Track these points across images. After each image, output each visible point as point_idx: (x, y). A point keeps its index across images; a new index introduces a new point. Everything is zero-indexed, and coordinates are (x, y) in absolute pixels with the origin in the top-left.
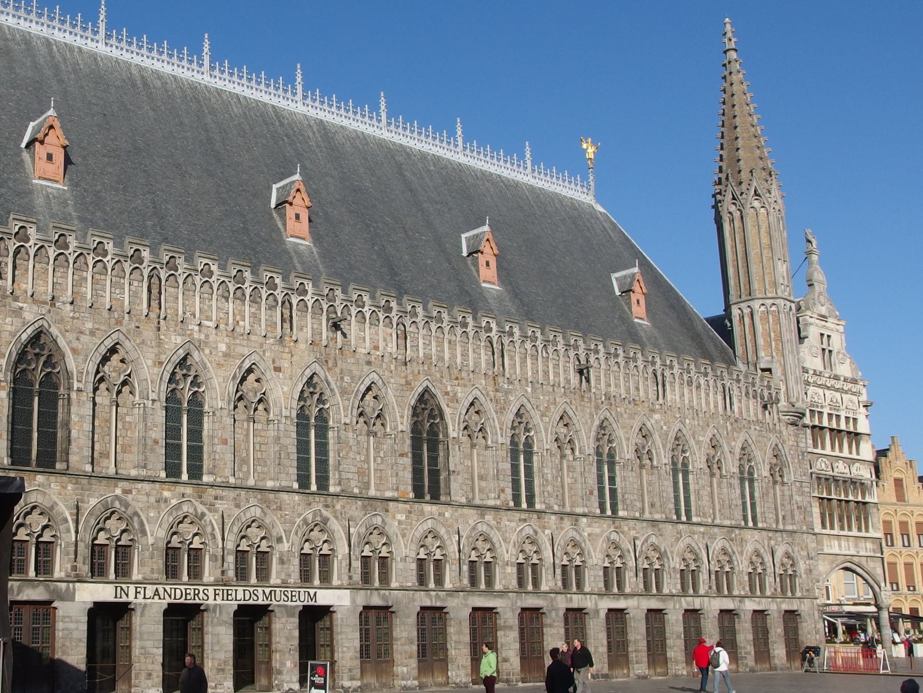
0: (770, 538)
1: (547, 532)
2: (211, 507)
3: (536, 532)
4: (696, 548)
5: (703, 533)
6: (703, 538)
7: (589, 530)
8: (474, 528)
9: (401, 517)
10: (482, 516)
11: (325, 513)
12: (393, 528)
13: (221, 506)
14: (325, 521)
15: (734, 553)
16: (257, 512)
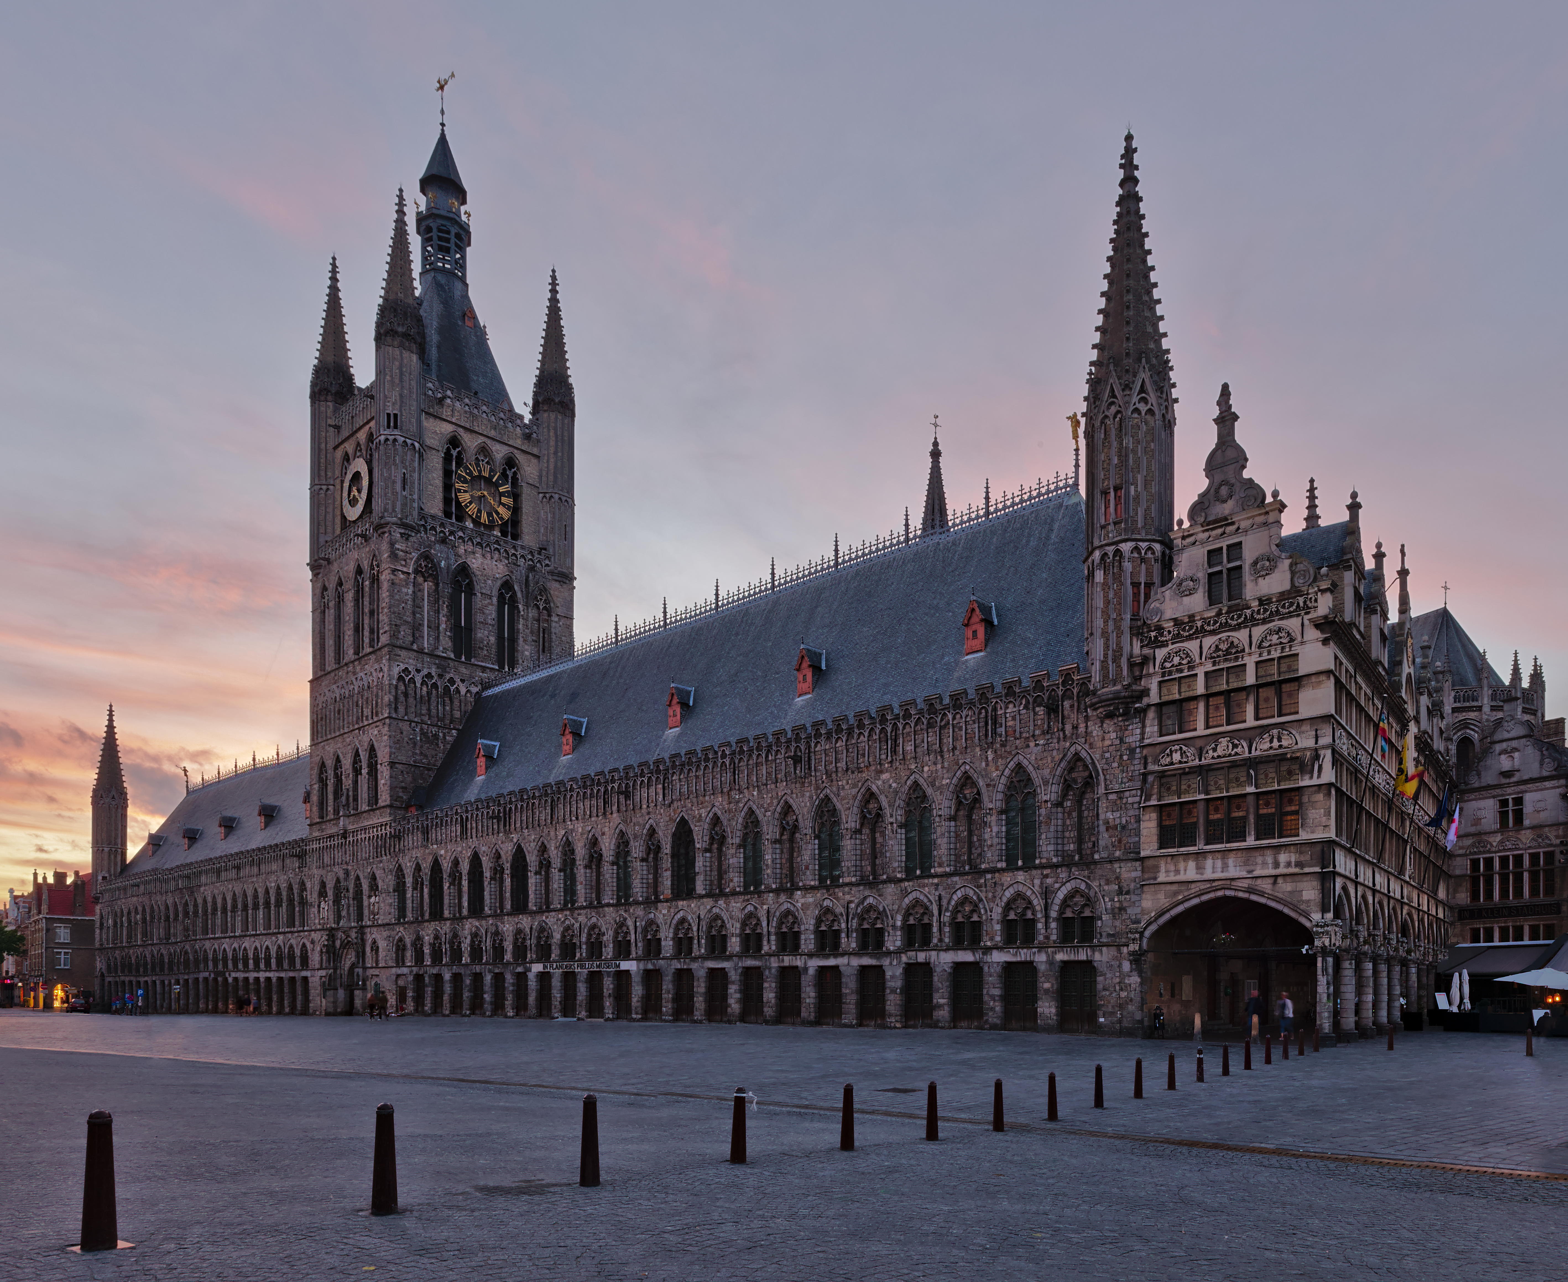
0: (1047, 876)
1: (765, 907)
2: (576, 920)
3: (756, 908)
4: (925, 900)
5: (937, 885)
6: (936, 889)
7: (803, 901)
8: (710, 911)
9: (665, 912)
10: (716, 901)
11: (626, 915)
12: (660, 919)
13: (580, 919)
14: (625, 919)
15: (981, 900)
16: (594, 920)
